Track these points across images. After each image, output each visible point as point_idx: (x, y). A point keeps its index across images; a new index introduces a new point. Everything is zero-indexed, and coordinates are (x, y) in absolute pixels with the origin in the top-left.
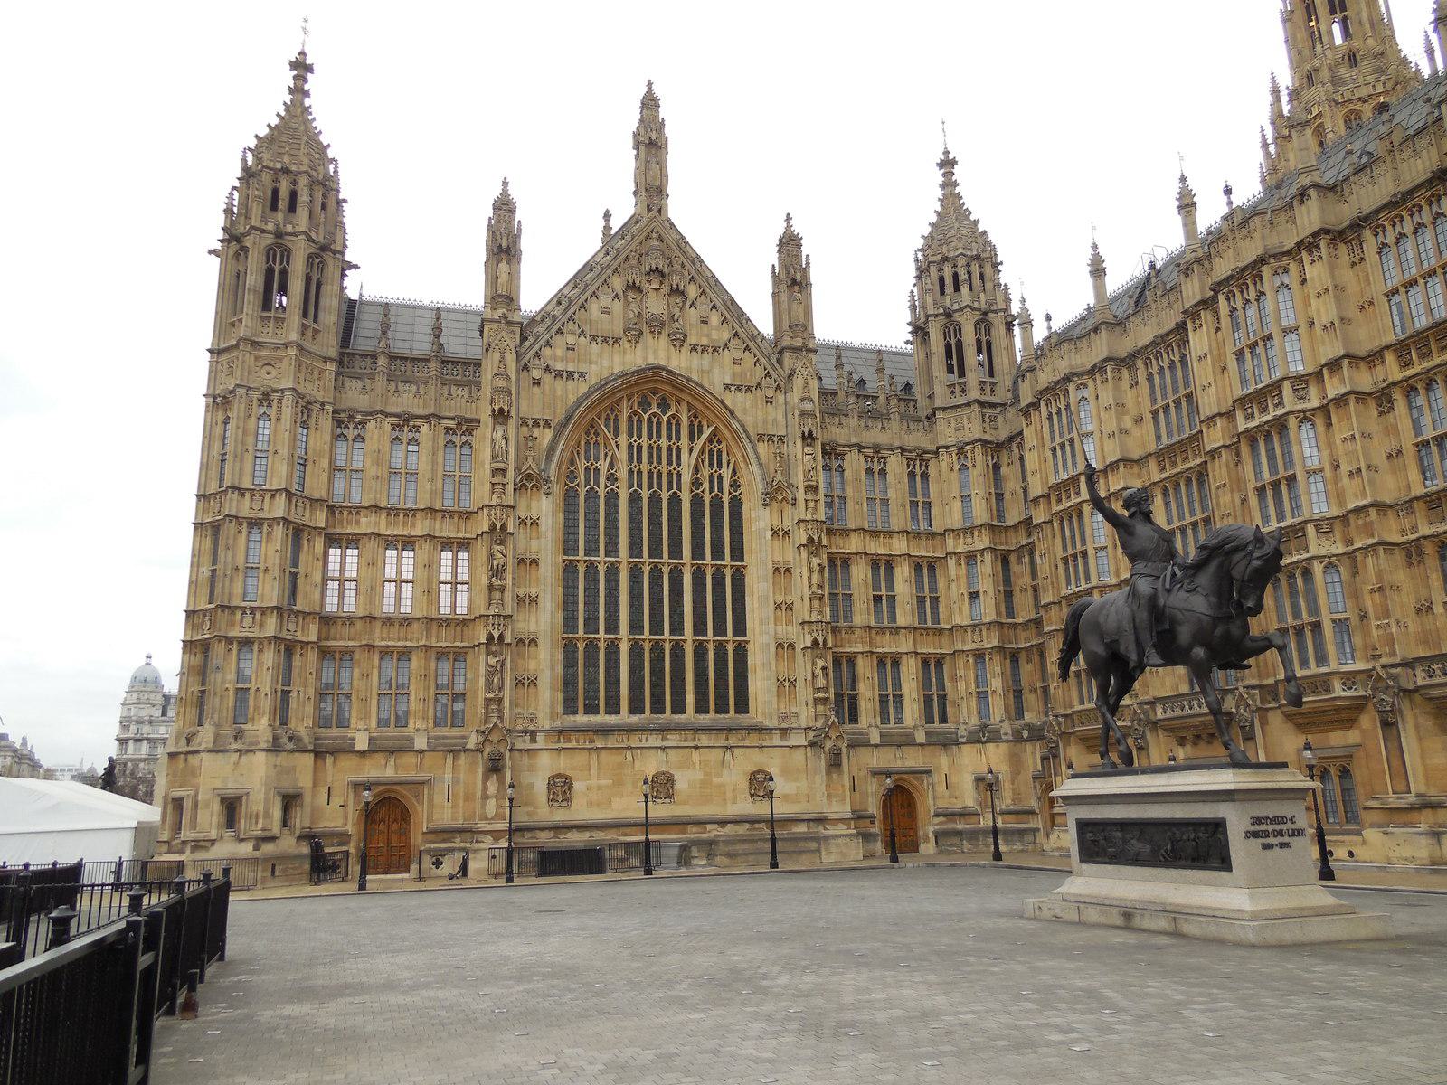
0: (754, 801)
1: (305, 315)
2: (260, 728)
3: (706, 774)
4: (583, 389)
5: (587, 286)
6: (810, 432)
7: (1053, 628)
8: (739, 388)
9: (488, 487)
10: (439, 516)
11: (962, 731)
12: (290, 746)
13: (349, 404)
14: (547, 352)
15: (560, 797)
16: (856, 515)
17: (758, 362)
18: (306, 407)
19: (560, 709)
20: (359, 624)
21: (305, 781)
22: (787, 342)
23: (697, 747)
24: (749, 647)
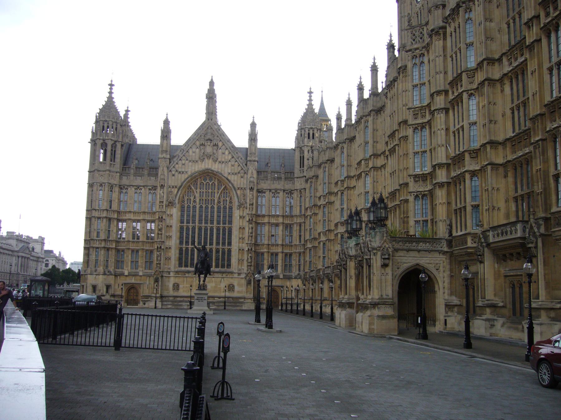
0: (229, 292)
1: (111, 161)
2: (101, 269)
4: (186, 176)
6: (252, 188)
8: (233, 174)
9: (158, 206)
10: (147, 213)
12: (108, 274)
14: (177, 166)
17: (239, 165)
18: (111, 187)
20: (126, 243)
24: (232, 250)
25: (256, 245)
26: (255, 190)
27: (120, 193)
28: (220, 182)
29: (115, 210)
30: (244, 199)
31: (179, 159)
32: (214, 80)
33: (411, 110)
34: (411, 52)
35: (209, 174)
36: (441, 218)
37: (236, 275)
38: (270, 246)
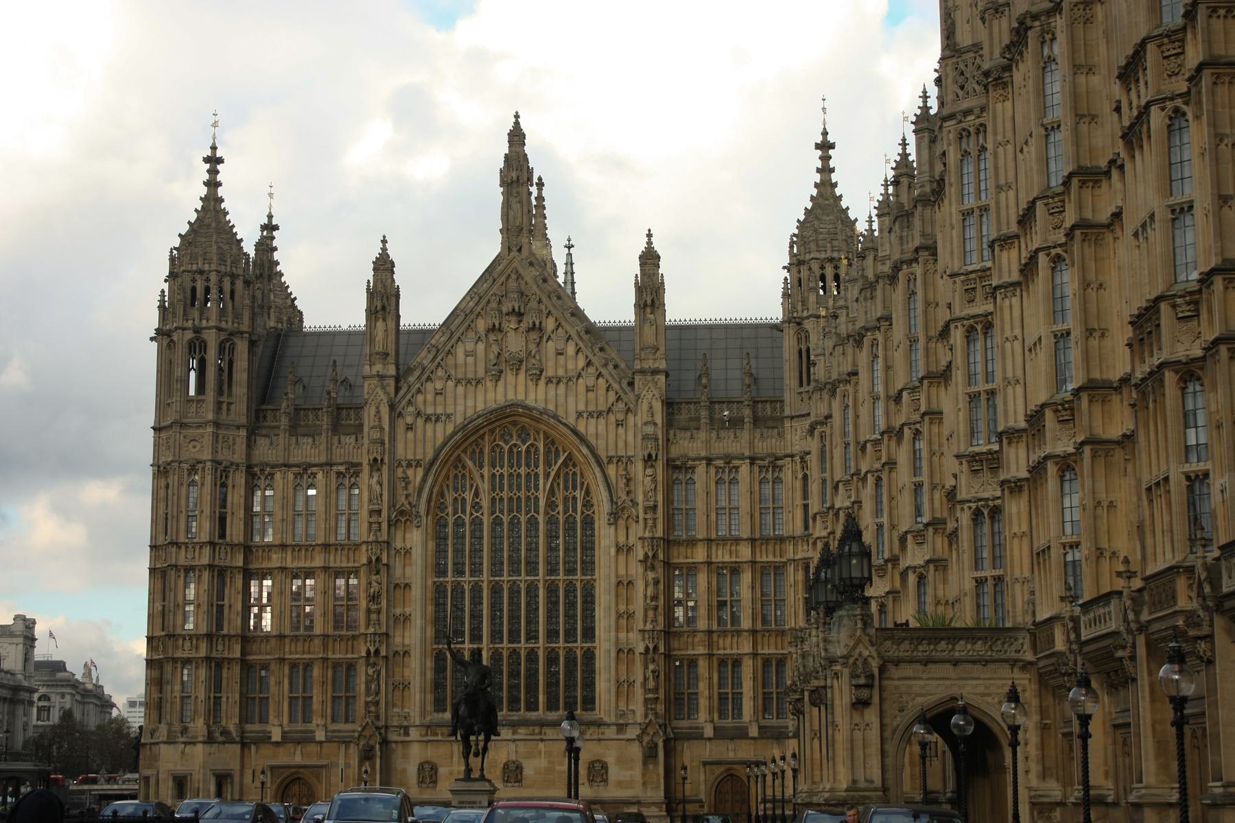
0: (591, 786)
2: (199, 726)
3: (549, 762)
4: (450, 428)
5: (452, 333)
9: (365, 526)
12: (221, 739)
14: (420, 398)
15: (428, 780)
20: (273, 642)
21: (235, 765)
23: (542, 740)
24: (597, 652)
25: (669, 632)
26: (660, 466)
28: (550, 442)
30: (628, 493)
31: (425, 376)
32: (523, 126)
33: (957, 279)
34: (953, 122)
35: (517, 418)
36: (1017, 574)
37: (611, 732)
38: (715, 636)
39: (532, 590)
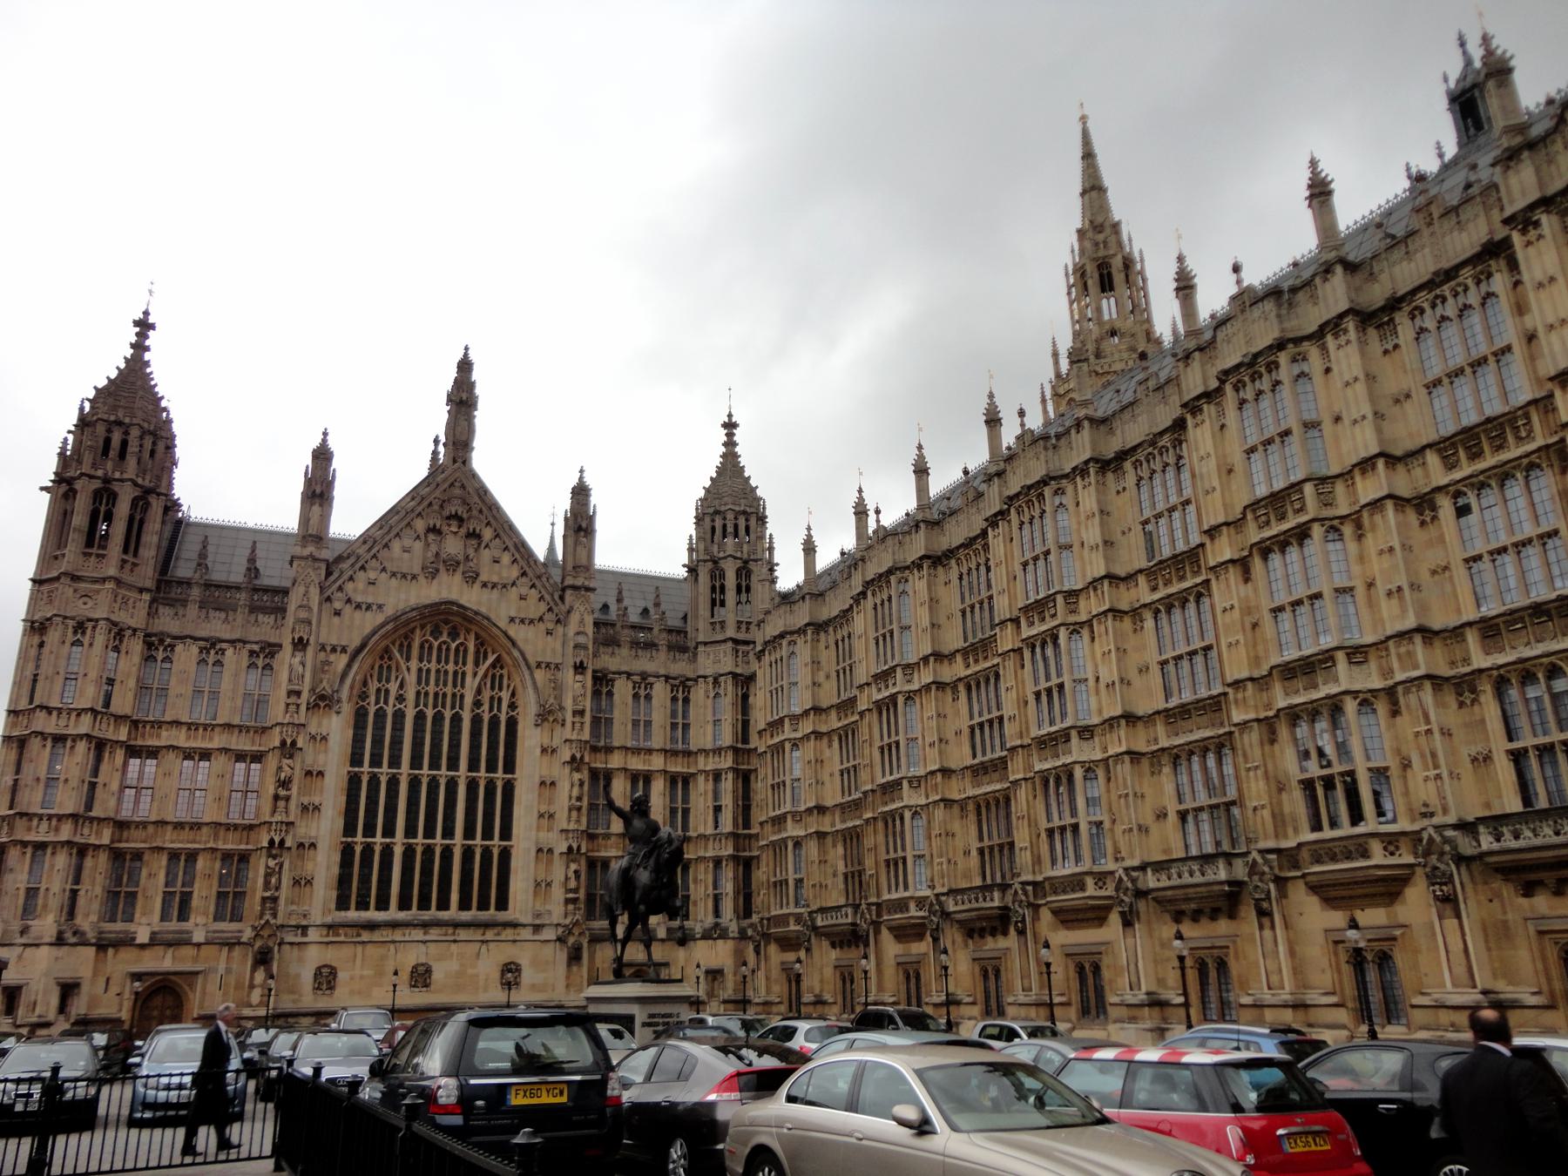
1: (126, 550)
2: (46, 925)
4: (380, 618)
5: (391, 527)
6: (582, 662)
7: (764, 843)
8: (522, 621)
9: (282, 706)
11: (698, 929)
12: (73, 940)
13: (160, 628)
14: (349, 586)
15: (324, 987)
16: (621, 734)
17: (541, 598)
18: (119, 633)
19: (333, 906)
20: (151, 829)
22: (569, 582)
23: (455, 941)
24: (514, 852)
27: (149, 658)
28: (481, 643)
29: (120, 713)
30: (555, 698)
31: (359, 565)
37: (526, 934)
39: (452, 785)
